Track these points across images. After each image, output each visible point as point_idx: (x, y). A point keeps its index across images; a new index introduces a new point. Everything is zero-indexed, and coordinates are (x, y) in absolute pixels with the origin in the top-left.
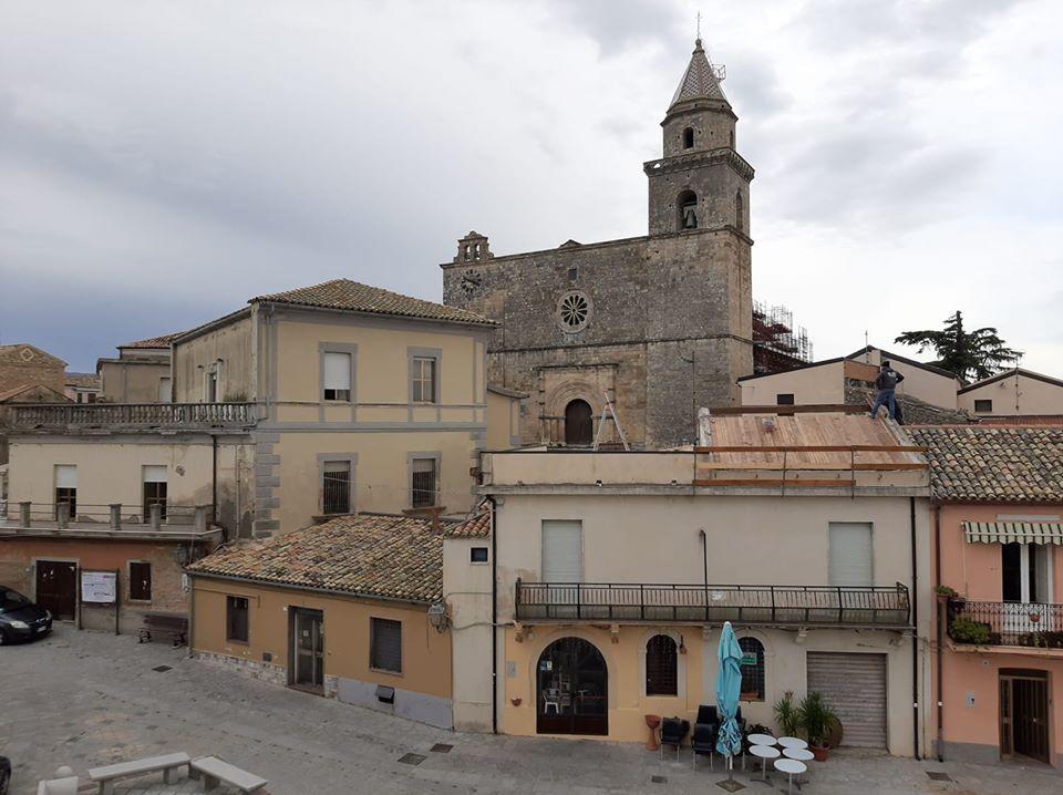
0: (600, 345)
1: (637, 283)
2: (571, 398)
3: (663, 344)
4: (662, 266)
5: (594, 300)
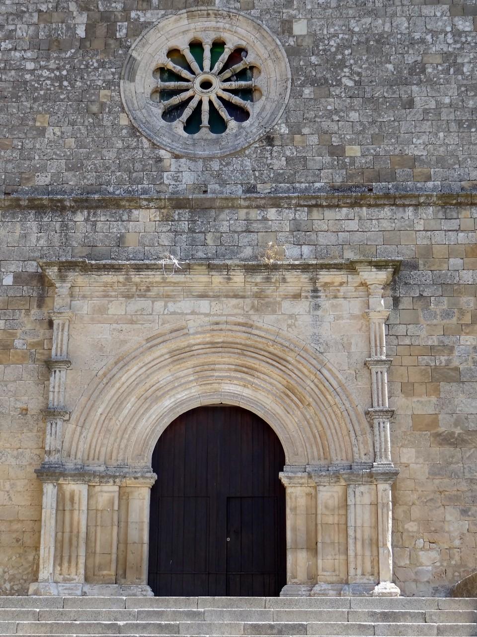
0: (312, 202)
2: (189, 395)
5: (293, 52)
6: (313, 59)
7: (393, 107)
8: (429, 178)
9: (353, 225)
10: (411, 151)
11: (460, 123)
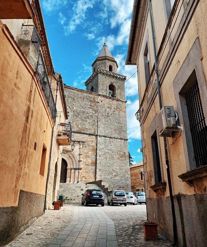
1: (94, 110)
3: (104, 138)
4: (104, 107)
5: (74, 111)
6: (76, 113)
7: (85, 121)
8: (88, 131)
9: (79, 136)
10: (86, 127)
11: (92, 125)
